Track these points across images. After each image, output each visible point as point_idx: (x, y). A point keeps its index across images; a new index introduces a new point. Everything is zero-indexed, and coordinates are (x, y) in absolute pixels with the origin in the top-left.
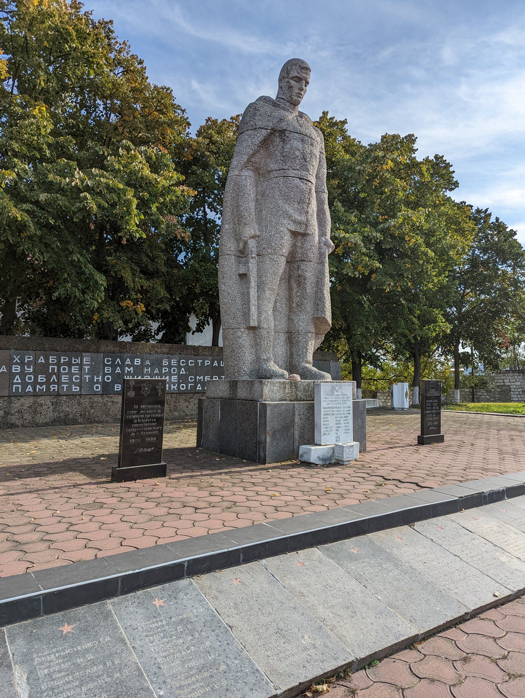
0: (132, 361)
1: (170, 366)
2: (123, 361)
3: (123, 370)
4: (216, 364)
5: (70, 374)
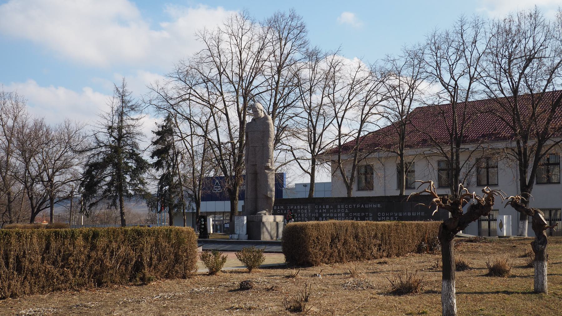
0: (325, 207)
1: (341, 208)
2: (322, 207)
3: (322, 211)
4: (363, 206)
5: (304, 213)
